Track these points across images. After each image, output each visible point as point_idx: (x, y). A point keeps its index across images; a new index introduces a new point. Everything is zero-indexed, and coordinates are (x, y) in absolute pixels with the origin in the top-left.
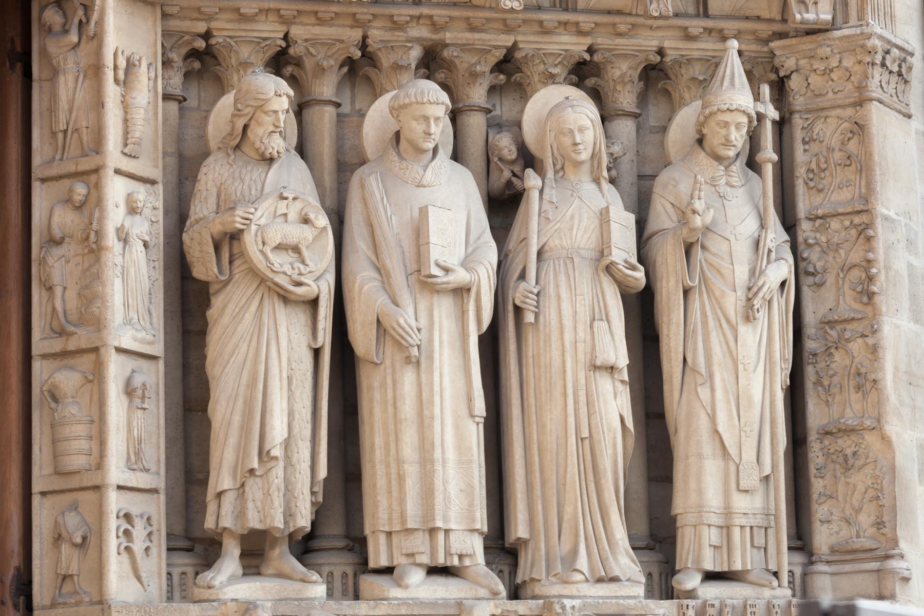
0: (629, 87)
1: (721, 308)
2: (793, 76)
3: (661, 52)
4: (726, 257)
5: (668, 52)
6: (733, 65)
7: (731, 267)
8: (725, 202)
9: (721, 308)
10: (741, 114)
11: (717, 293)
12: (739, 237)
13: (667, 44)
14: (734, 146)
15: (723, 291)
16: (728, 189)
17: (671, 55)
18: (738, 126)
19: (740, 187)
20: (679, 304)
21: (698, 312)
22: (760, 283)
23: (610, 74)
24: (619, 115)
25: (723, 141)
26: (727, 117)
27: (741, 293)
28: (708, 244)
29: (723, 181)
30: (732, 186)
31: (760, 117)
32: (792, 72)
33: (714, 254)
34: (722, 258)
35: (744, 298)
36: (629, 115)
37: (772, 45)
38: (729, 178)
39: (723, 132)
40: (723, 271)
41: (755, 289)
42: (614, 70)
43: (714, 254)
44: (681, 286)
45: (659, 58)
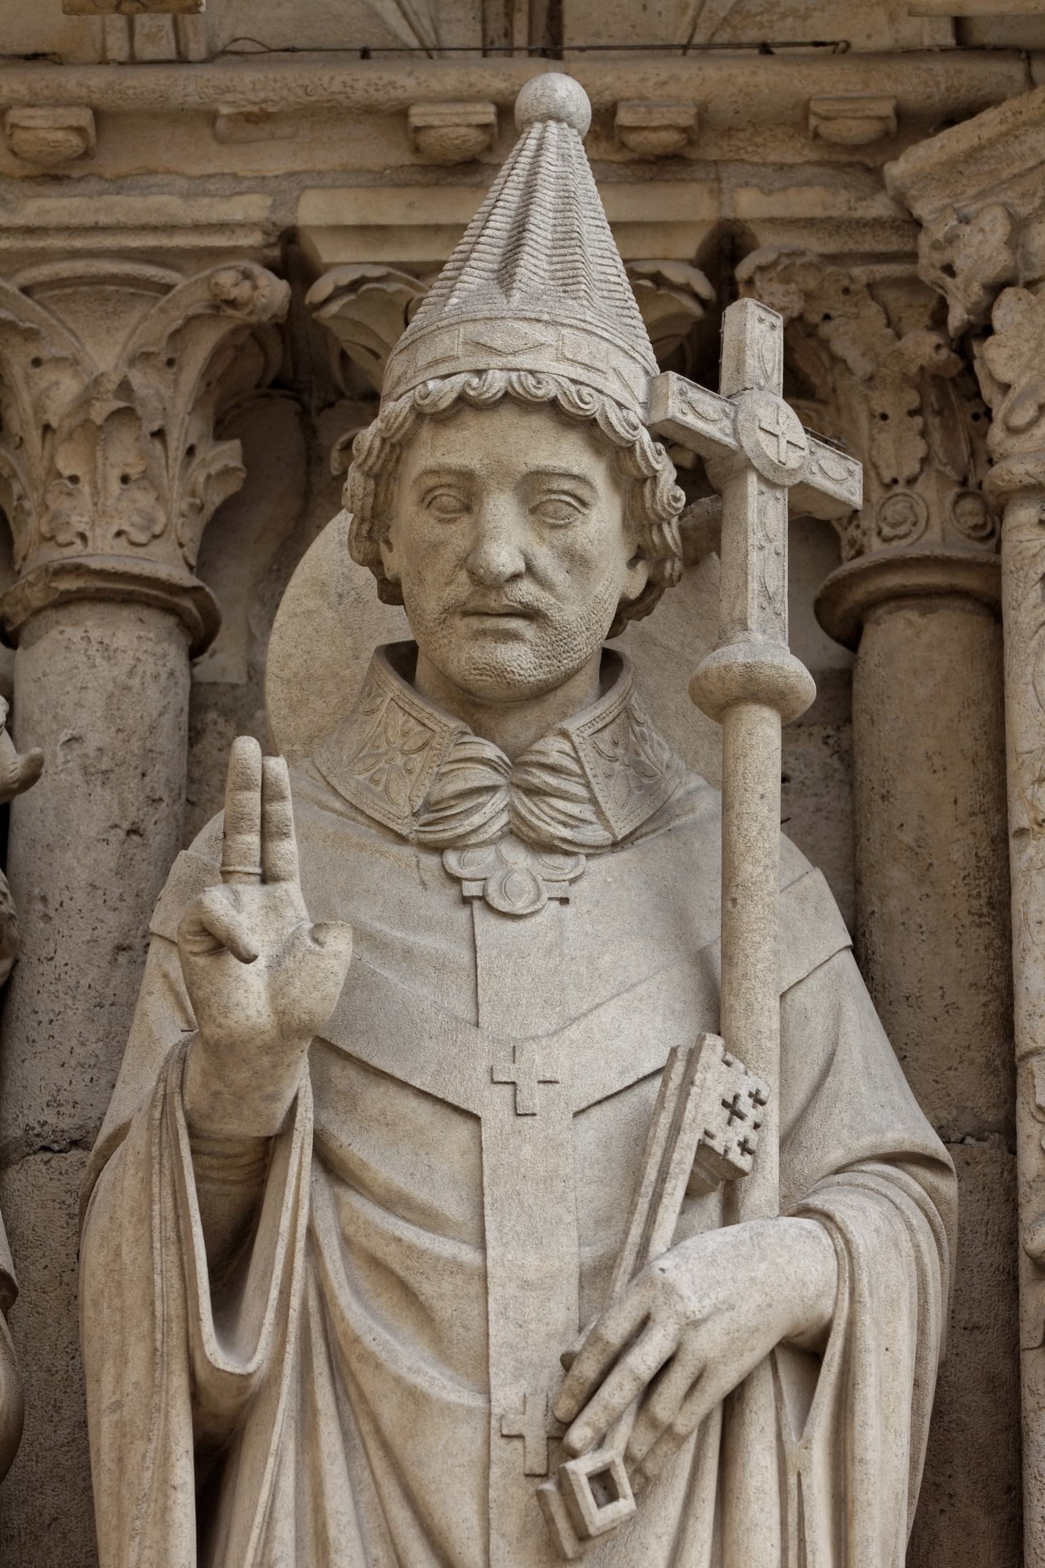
0: (123, 452)
1: (411, 1498)
2: (999, 317)
3: (290, 256)
4: (452, 1205)
5: (326, 251)
6: (529, 191)
7: (469, 1255)
8: (486, 925)
9: (411, 1498)
10: (538, 421)
11: (389, 1412)
12: (534, 1097)
13: (312, 211)
14: (530, 614)
15: (415, 1398)
16: (518, 857)
17: (341, 261)
18: (542, 497)
19: (595, 851)
20: (165, 1485)
21: (285, 1530)
22: (616, 1328)
23: (26, 399)
24: (66, 601)
25: (462, 588)
26: (461, 449)
27: (519, 1394)
28: (356, 1146)
29: (491, 814)
30: (543, 846)
31: (705, 473)
32: (995, 289)
33: (392, 1202)
34: (428, 1219)
35: (534, 1428)
36: (126, 600)
37: (897, 170)
38: (526, 805)
39: (457, 536)
40: (427, 1289)
41: (588, 1368)
42: (46, 376)
43: (392, 1202)
44: (179, 1383)
45: (274, 291)
